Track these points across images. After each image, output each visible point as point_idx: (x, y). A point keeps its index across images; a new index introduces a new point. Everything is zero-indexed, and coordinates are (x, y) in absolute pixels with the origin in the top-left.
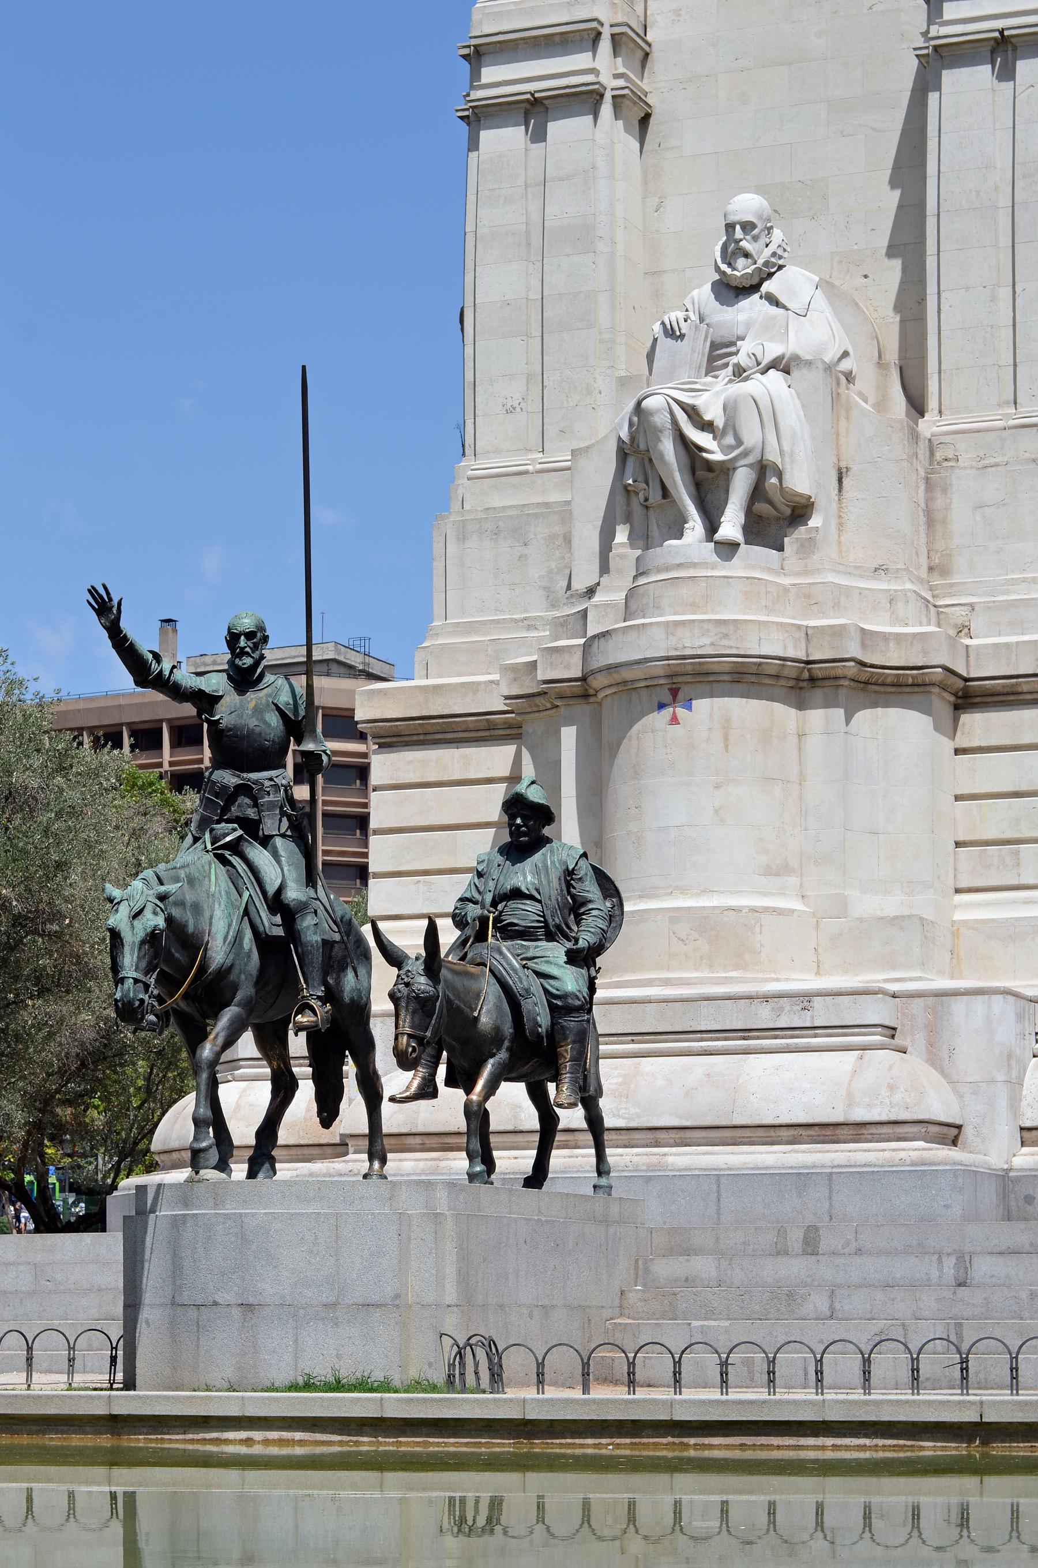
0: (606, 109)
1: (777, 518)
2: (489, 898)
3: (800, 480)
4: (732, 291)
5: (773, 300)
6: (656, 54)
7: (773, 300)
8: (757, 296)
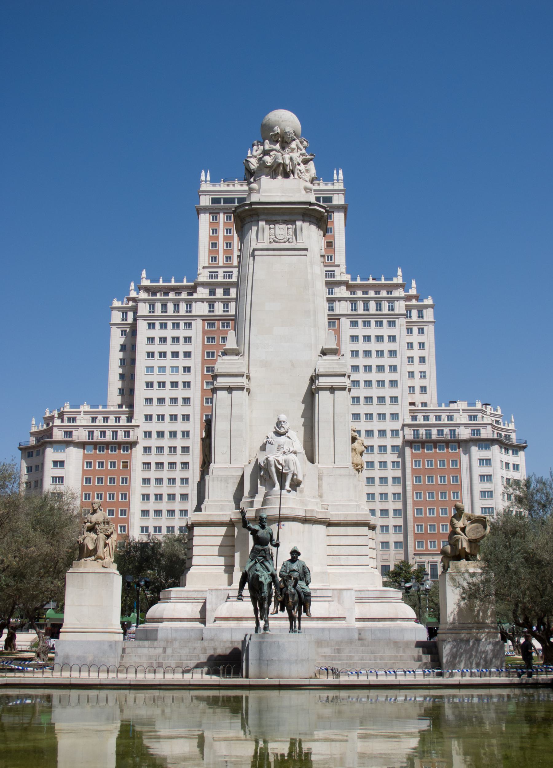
0: (245, 390)
2: (288, 571)
3: (300, 478)
4: (278, 434)
5: (288, 437)
6: (251, 378)
7: (288, 437)
8: (284, 436)
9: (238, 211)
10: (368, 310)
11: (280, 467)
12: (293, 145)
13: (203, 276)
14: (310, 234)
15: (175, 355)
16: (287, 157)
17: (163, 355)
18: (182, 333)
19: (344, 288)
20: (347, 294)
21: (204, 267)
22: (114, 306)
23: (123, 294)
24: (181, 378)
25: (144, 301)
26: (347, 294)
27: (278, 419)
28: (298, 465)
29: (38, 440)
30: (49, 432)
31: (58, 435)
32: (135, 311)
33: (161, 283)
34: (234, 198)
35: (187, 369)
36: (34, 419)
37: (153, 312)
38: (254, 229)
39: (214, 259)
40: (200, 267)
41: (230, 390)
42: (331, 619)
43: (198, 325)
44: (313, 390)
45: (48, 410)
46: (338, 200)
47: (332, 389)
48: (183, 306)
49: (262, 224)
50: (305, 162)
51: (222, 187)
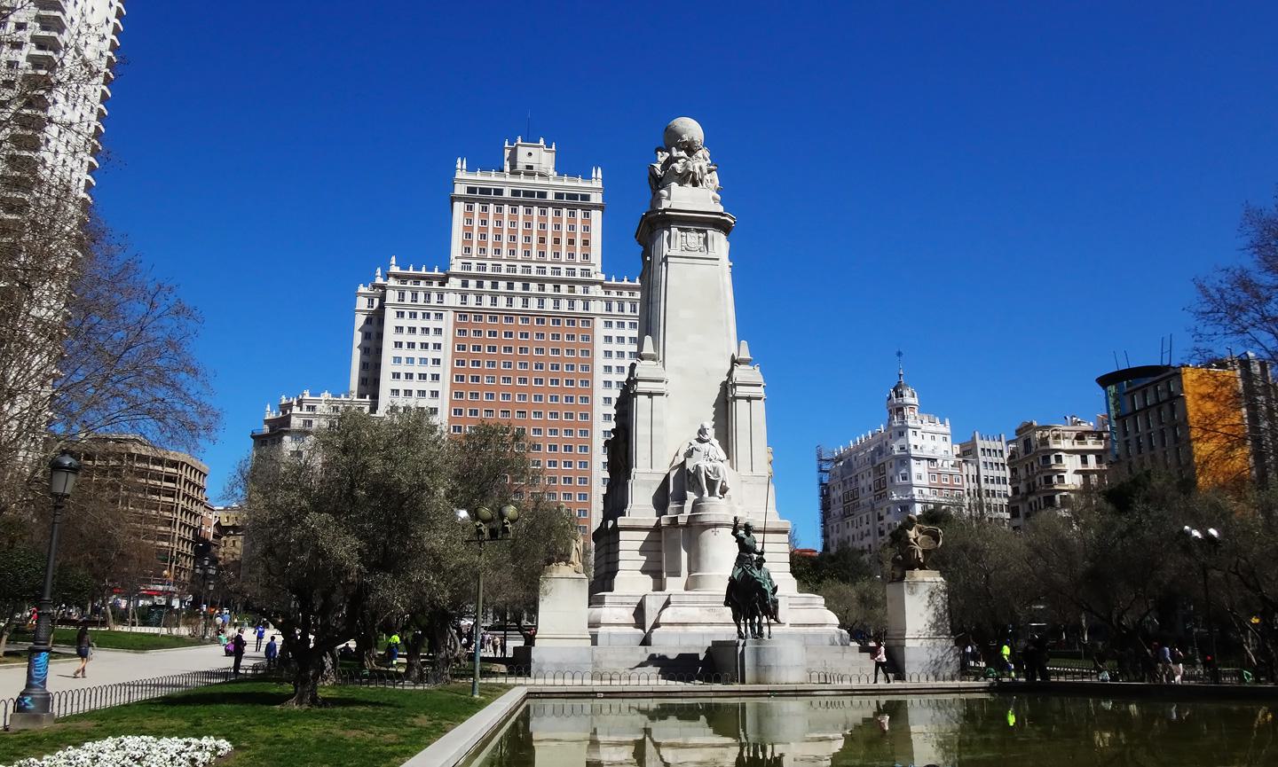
3: (728, 486)
9: (650, 216)
10: (623, 311)
11: (709, 473)
12: (700, 154)
13: (456, 267)
14: (720, 244)
15: (425, 346)
16: (697, 165)
17: (411, 345)
18: (432, 323)
19: (599, 287)
20: (603, 295)
21: (456, 258)
22: (359, 291)
23: (368, 279)
24: (430, 369)
25: (393, 288)
26: (603, 295)
27: (702, 426)
28: (726, 474)
29: (272, 429)
30: (286, 421)
31: (296, 423)
32: (383, 299)
33: (411, 271)
34: (491, 189)
35: (437, 362)
36: (269, 406)
37: (416, 301)
38: (666, 233)
40: (452, 257)
41: (650, 395)
43: (449, 316)
44: (729, 399)
45: (284, 397)
46: (596, 198)
47: (749, 399)
48: (434, 297)
49: (674, 230)
50: (710, 171)
51: (479, 176)
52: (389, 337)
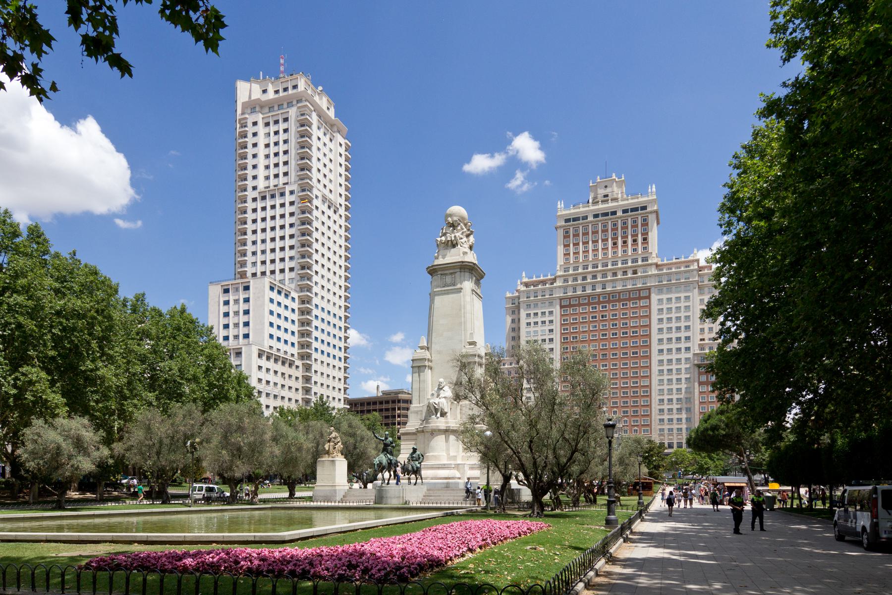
1: (443, 414)
3: (446, 410)
15: (544, 322)
19: (654, 267)
25: (523, 291)
26: (656, 272)
39: (567, 259)
42: (449, 478)
52: (524, 320)
